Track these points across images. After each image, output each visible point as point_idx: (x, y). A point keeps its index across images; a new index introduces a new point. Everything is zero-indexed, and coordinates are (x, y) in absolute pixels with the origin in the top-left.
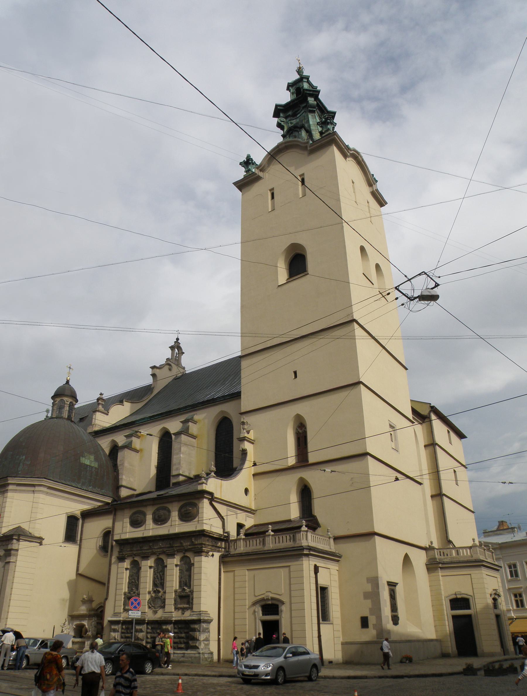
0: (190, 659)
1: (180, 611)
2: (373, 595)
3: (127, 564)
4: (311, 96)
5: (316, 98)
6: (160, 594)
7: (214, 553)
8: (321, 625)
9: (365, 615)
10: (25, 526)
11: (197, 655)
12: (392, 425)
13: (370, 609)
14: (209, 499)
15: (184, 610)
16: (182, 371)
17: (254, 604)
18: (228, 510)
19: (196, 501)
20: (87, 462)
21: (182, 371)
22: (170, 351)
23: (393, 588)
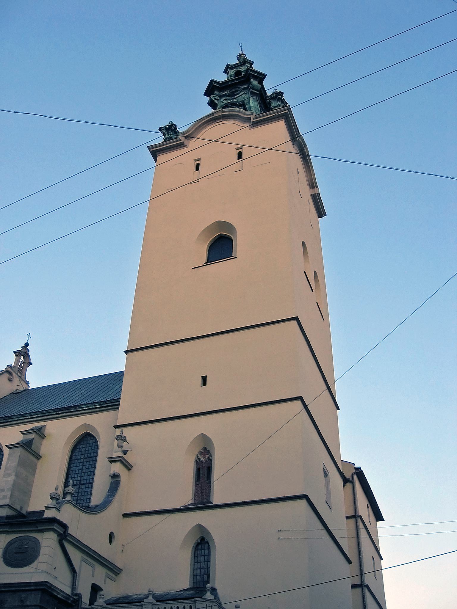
4: (255, 78)
5: (261, 81)
14: (59, 535)
16: (25, 386)
18: (83, 560)
21: (25, 386)
22: (14, 357)
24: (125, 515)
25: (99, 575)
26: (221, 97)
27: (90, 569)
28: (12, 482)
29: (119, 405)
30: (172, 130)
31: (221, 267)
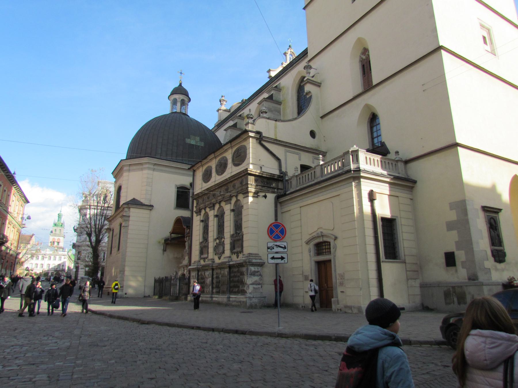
0: (239, 304)
2: (461, 225)
3: (201, 217)
6: (223, 239)
7: (267, 194)
8: (383, 265)
9: (450, 249)
10: (138, 198)
11: (244, 300)
12: (483, 23)
13: (457, 243)
15: (237, 254)
17: (307, 243)
18: (286, 152)
19: (244, 143)
20: (193, 142)
23: (494, 215)
24: (322, 117)
25: (307, 159)
27: (297, 157)
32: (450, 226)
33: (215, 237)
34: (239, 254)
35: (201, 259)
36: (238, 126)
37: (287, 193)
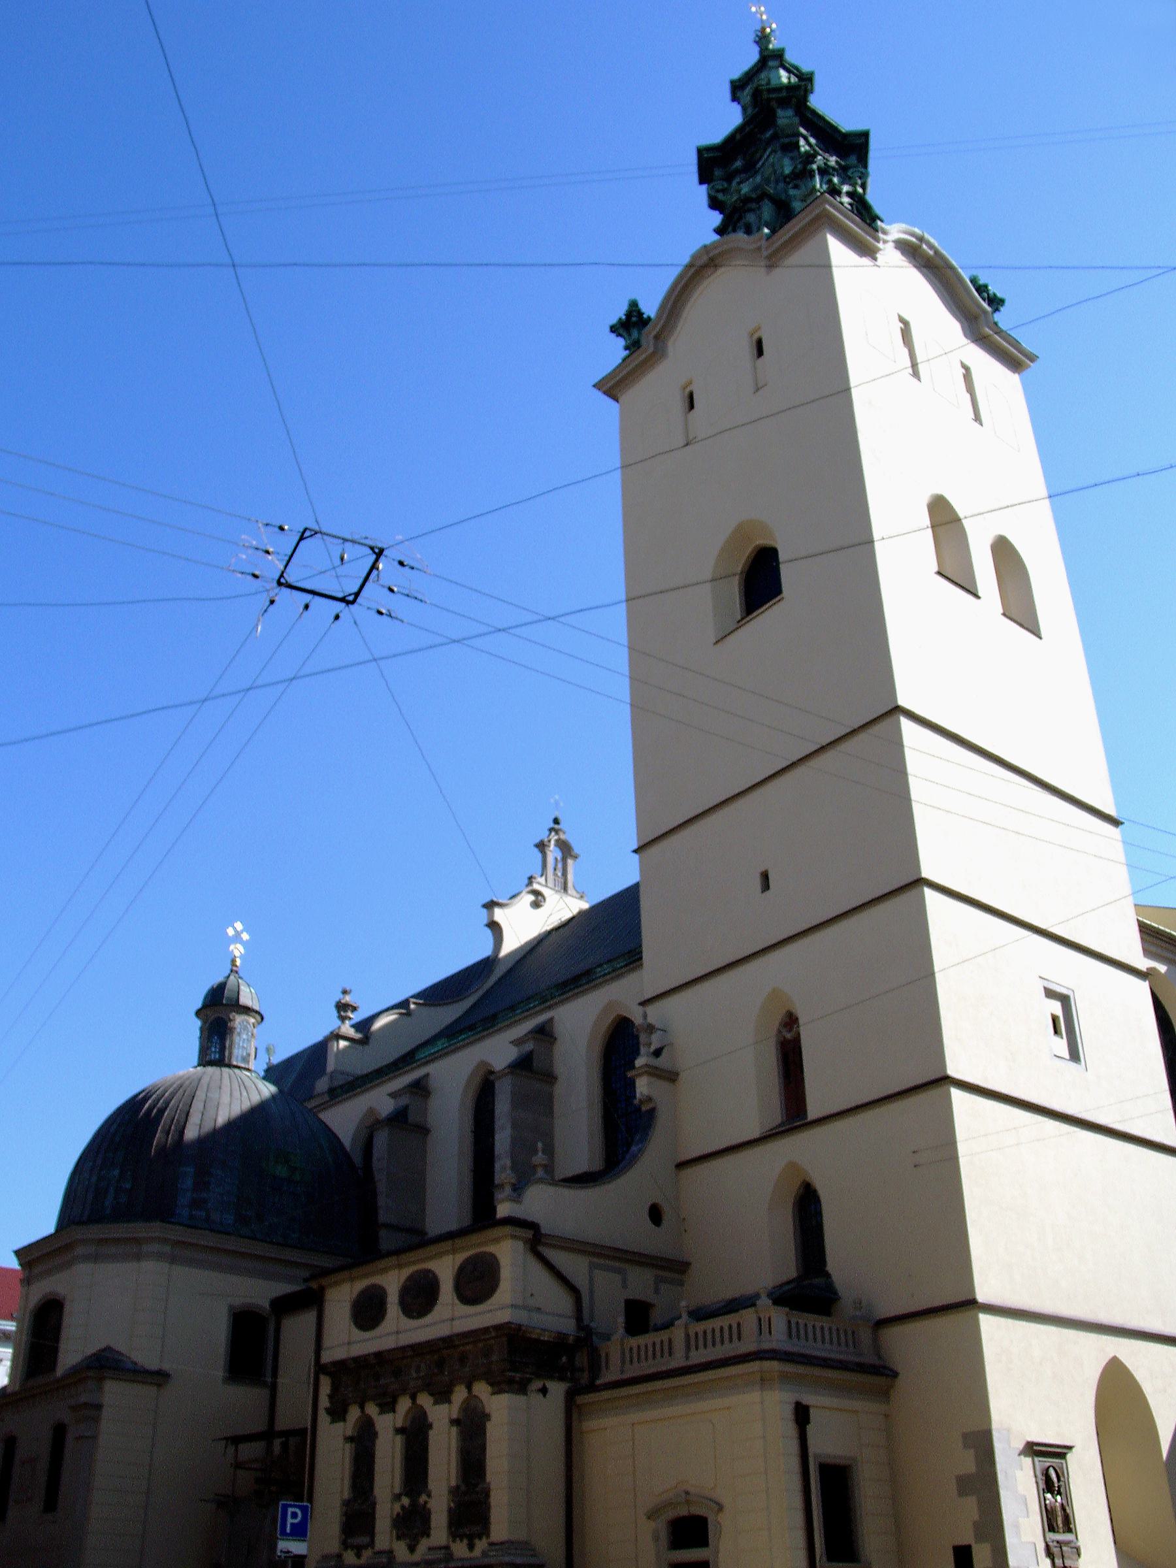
1: (465, 1541)
3: (349, 1426)
4: (784, 103)
6: (423, 1498)
7: (550, 1385)
10: (121, 1346)
13: (975, 1523)
17: (652, 1515)
25: (640, 1284)
26: (729, 179)
28: (509, 1140)
29: (641, 958)
30: (635, 324)
31: (770, 617)
32: (965, 1485)
33: (397, 1490)
34: (477, 1541)
35: (346, 1549)
36: (411, 1119)
37: (598, 1382)
